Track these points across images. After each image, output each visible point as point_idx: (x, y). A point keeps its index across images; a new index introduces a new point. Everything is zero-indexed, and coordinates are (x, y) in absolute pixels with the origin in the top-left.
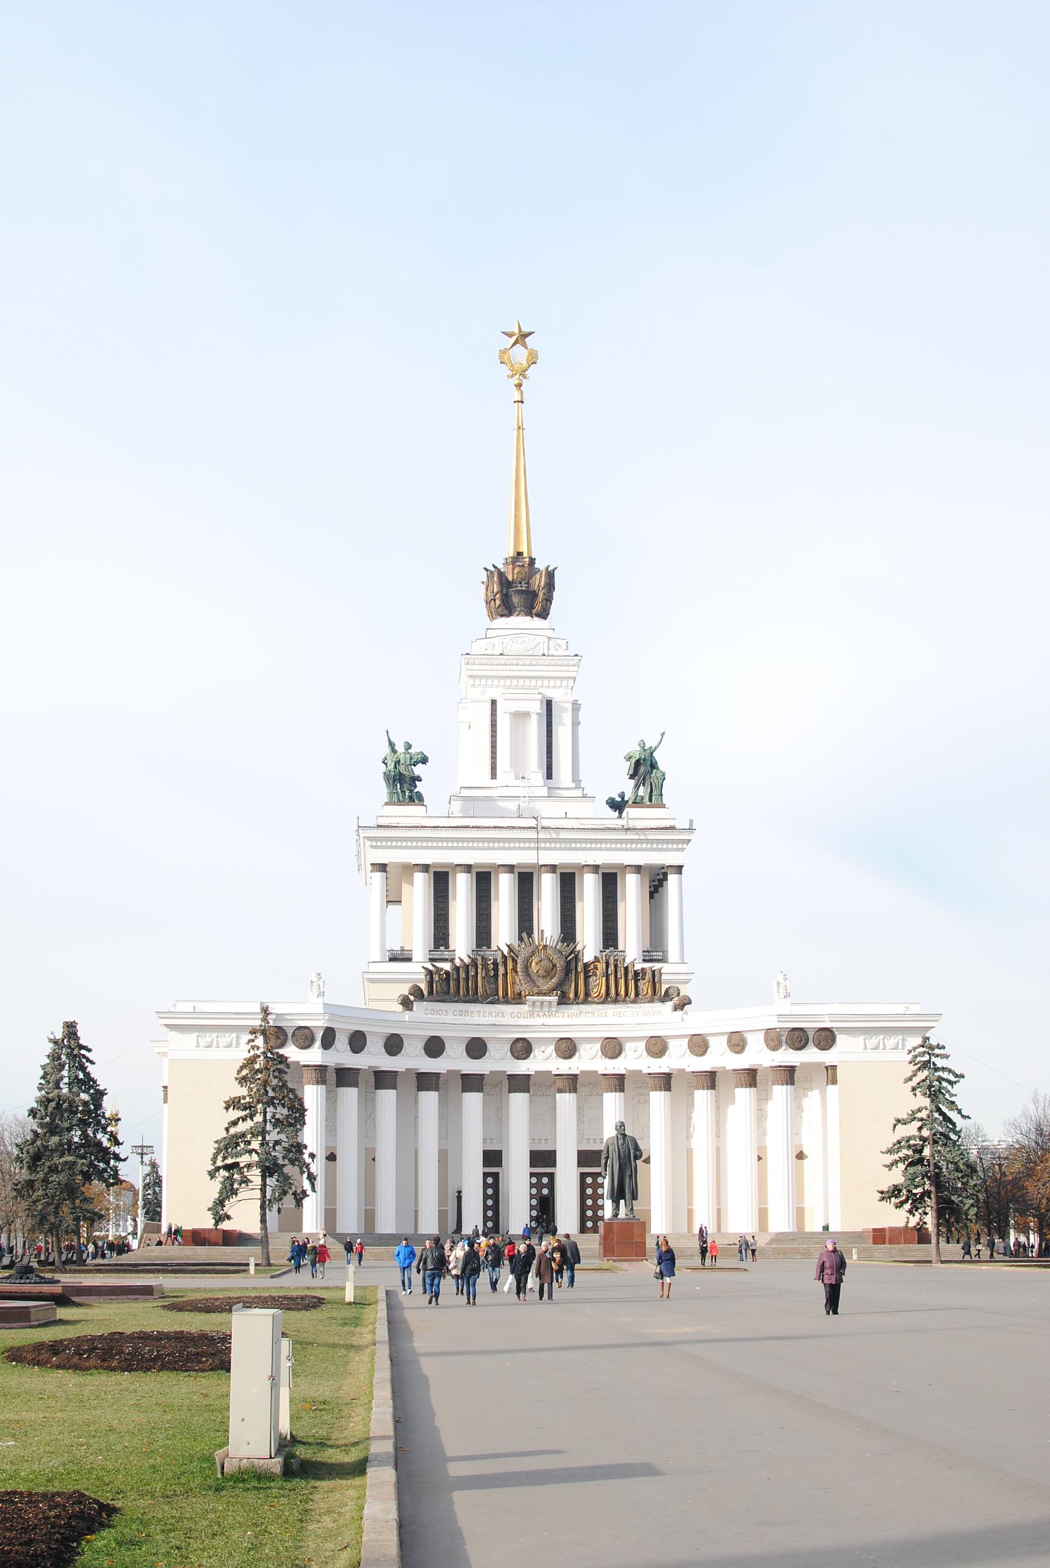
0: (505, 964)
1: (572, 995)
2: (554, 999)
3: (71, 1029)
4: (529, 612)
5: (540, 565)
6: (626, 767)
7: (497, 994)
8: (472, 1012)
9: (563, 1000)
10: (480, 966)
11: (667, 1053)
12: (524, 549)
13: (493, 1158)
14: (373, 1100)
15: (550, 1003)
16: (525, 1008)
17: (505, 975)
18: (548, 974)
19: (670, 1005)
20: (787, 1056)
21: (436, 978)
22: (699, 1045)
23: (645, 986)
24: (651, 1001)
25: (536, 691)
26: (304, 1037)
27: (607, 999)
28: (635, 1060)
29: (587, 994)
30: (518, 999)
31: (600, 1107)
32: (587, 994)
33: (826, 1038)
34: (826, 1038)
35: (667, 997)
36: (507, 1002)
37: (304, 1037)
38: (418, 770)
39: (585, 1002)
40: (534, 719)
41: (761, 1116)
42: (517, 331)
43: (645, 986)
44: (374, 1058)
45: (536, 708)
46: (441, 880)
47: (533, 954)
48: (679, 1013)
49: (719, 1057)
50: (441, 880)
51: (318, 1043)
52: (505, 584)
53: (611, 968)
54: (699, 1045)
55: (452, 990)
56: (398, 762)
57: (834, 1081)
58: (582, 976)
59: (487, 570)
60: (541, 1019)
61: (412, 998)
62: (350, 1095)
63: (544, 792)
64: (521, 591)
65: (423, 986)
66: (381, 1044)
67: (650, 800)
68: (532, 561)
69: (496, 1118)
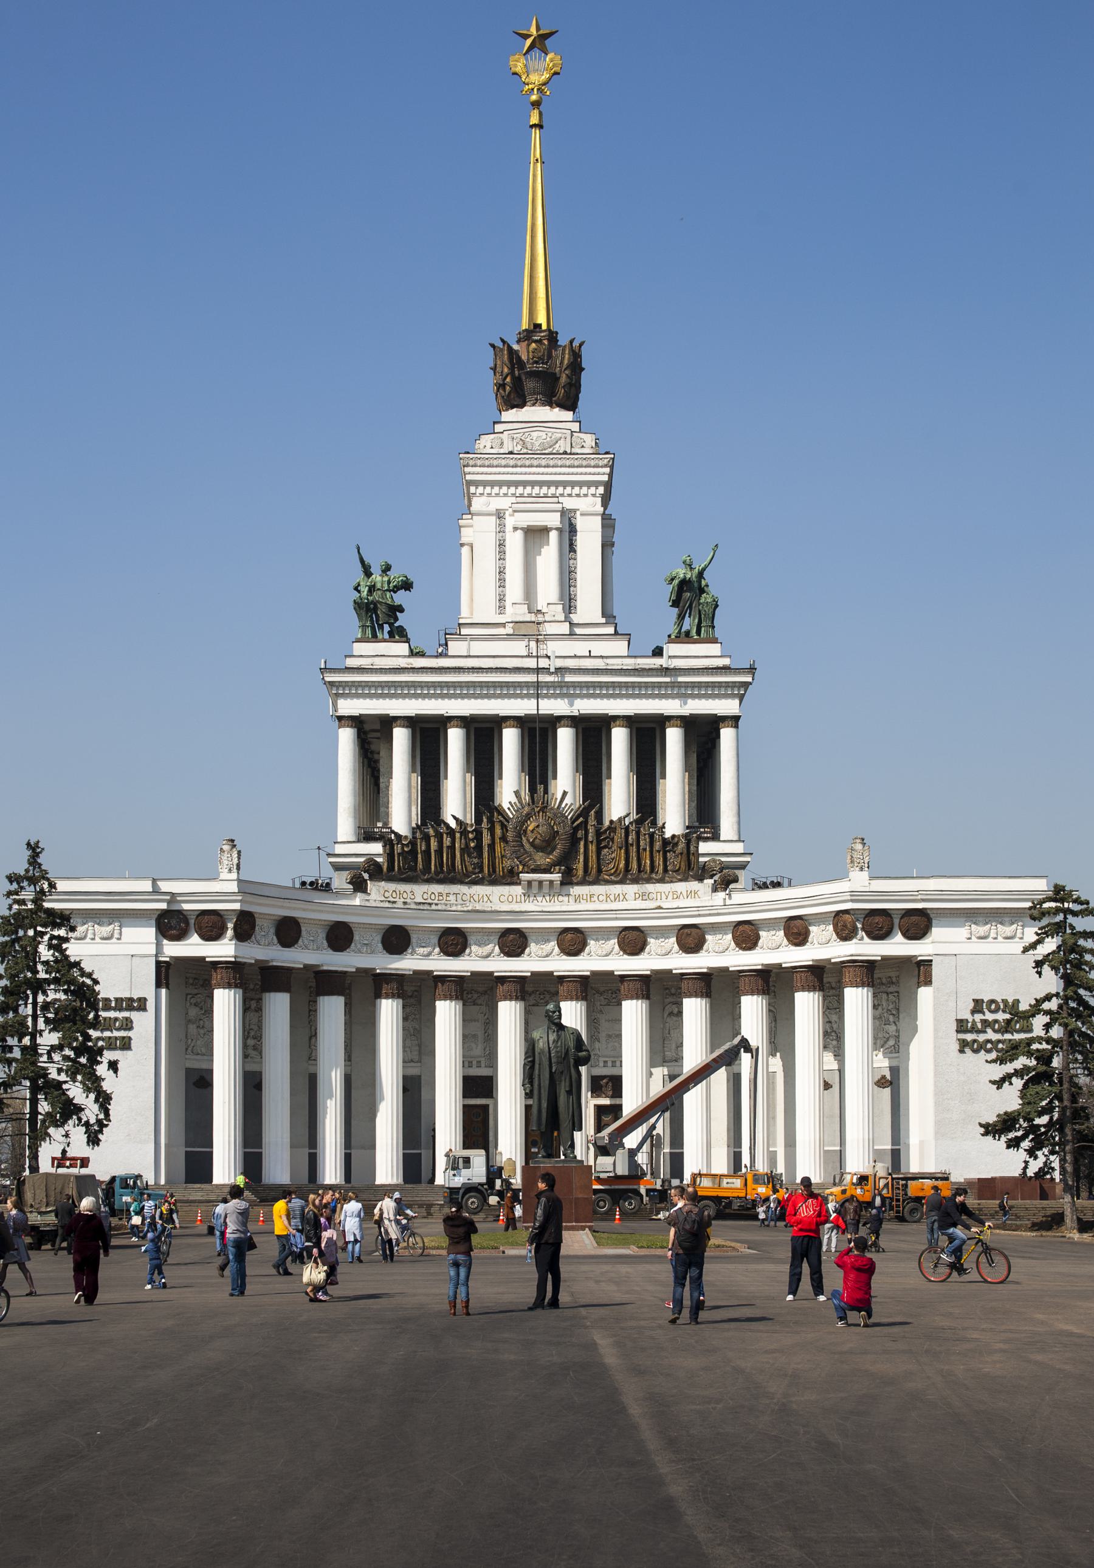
0: (492, 830)
1: (581, 872)
2: (556, 877)
4: (550, 401)
5: (563, 341)
6: (667, 591)
7: (481, 871)
8: (448, 895)
10: (458, 835)
11: (705, 947)
12: (541, 319)
13: (478, 1087)
15: (551, 882)
16: (518, 890)
17: (492, 846)
18: (546, 846)
21: (398, 849)
22: (746, 935)
23: (674, 860)
24: (685, 879)
25: (556, 500)
27: (625, 877)
28: (662, 957)
29: (599, 871)
30: (510, 878)
31: (619, 1021)
32: (599, 871)
33: (918, 923)
34: (918, 923)
36: (494, 882)
37: (211, 925)
38: (400, 598)
40: (553, 536)
41: (833, 1036)
42: (533, 30)
43: (674, 860)
45: (553, 520)
47: (528, 816)
48: (721, 895)
49: (775, 951)
51: (230, 933)
53: (632, 838)
54: (746, 935)
55: (420, 865)
56: (372, 589)
57: (928, 982)
58: (592, 848)
59: (493, 346)
61: (366, 876)
63: (565, 628)
64: (540, 374)
66: (322, 936)
67: (698, 633)
68: (552, 336)
69: (480, 1036)
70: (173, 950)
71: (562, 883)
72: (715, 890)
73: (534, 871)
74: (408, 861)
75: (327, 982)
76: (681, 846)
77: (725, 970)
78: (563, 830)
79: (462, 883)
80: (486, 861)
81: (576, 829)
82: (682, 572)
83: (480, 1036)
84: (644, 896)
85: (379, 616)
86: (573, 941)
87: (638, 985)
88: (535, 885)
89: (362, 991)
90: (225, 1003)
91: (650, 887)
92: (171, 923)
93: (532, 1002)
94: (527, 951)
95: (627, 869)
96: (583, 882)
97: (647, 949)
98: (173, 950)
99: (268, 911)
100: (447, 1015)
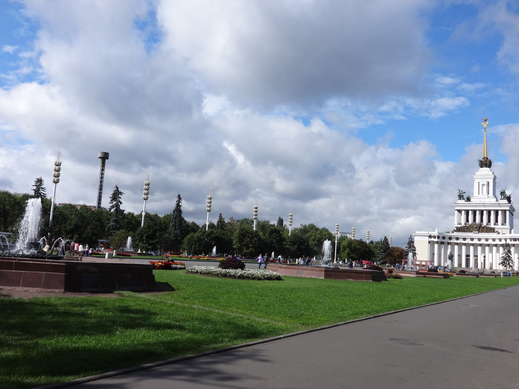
3: (385, 237)
6: (500, 193)
13: (468, 256)
18: (476, 228)
20: (513, 242)
26: (435, 237)
27: (486, 232)
30: (472, 232)
37: (435, 237)
38: (464, 194)
44: (447, 240)
45: (486, 183)
46: (467, 212)
50: (467, 212)
52: (481, 162)
60: (475, 235)
65: (455, 229)
69: (468, 250)
70: (430, 240)
74: (459, 230)
78: (478, 226)
82: (502, 191)
83: (468, 250)
85: (461, 197)
86: (479, 240)
89: (453, 245)
90: (436, 246)
92: (430, 237)
98: (430, 240)
99: (441, 236)
100: (464, 247)
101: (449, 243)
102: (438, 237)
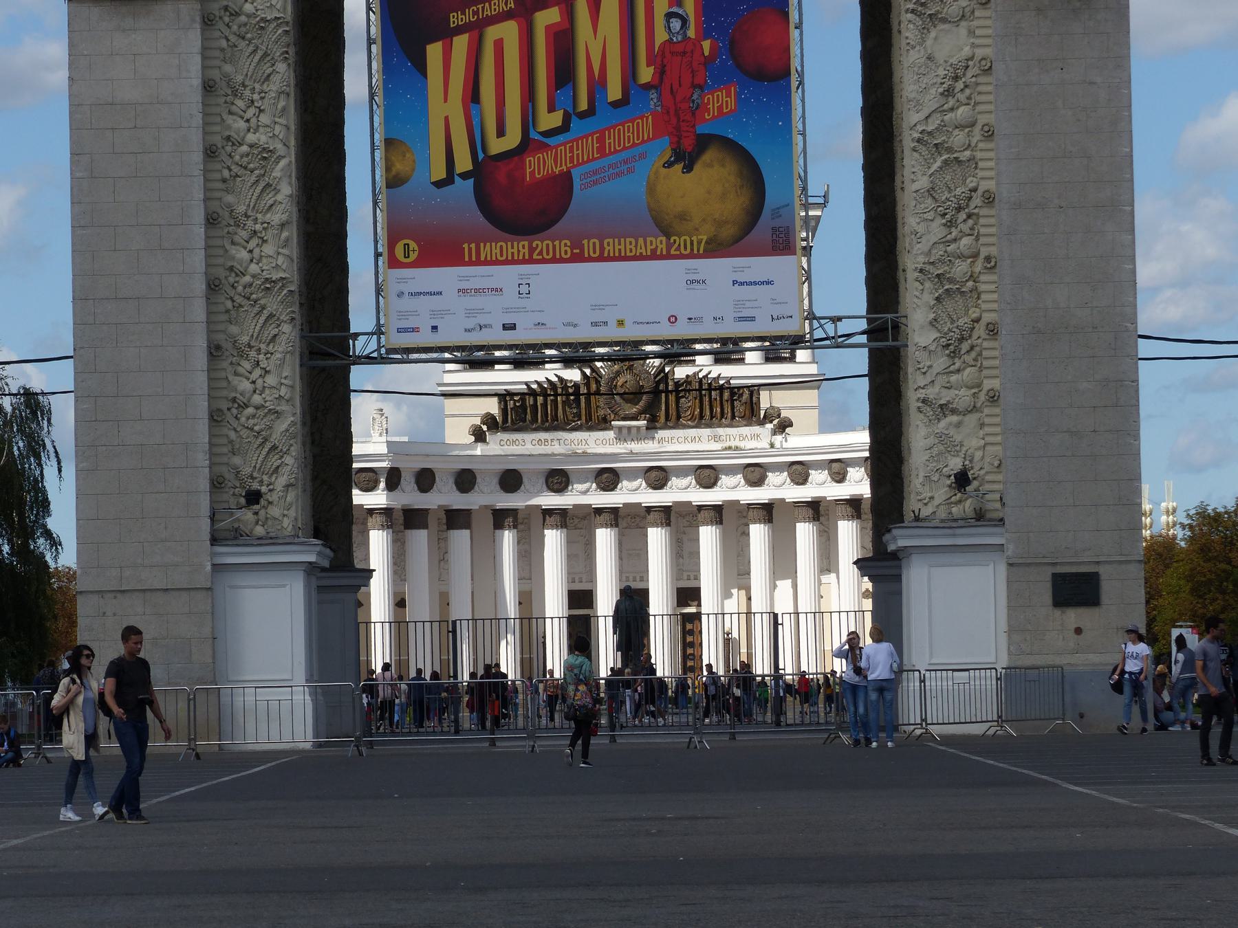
9: (653, 426)
13: (581, 599)
14: (446, 540)
15: (638, 428)
19: (769, 426)
21: (511, 404)
27: (700, 421)
30: (603, 424)
31: (696, 540)
35: (768, 418)
39: (676, 426)
44: (444, 496)
51: (382, 485)
58: (672, 398)
61: (485, 428)
62: (419, 539)
66: (451, 481)
71: (647, 428)
72: (774, 433)
73: (624, 419)
75: (456, 519)
76: (746, 396)
77: (783, 500)
79: (564, 430)
80: (583, 412)
81: (658, 383)
84: (717, 438)
86: (658, 477)
87: (712, 513)
88: (625, 431)
91: (721, 431)
93: (625, 525)
94: (619, 486)
95: (701, 417)
96: (665, 427)
97: (719, 483)
99: (409, 466)
100: (553, 540)
101: (456, 519)
102: (393, 479)
